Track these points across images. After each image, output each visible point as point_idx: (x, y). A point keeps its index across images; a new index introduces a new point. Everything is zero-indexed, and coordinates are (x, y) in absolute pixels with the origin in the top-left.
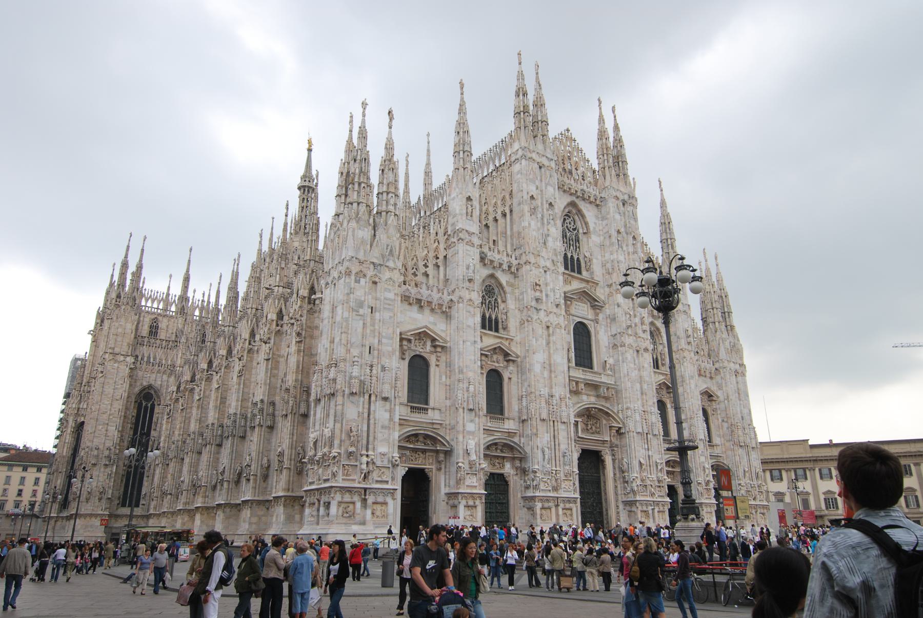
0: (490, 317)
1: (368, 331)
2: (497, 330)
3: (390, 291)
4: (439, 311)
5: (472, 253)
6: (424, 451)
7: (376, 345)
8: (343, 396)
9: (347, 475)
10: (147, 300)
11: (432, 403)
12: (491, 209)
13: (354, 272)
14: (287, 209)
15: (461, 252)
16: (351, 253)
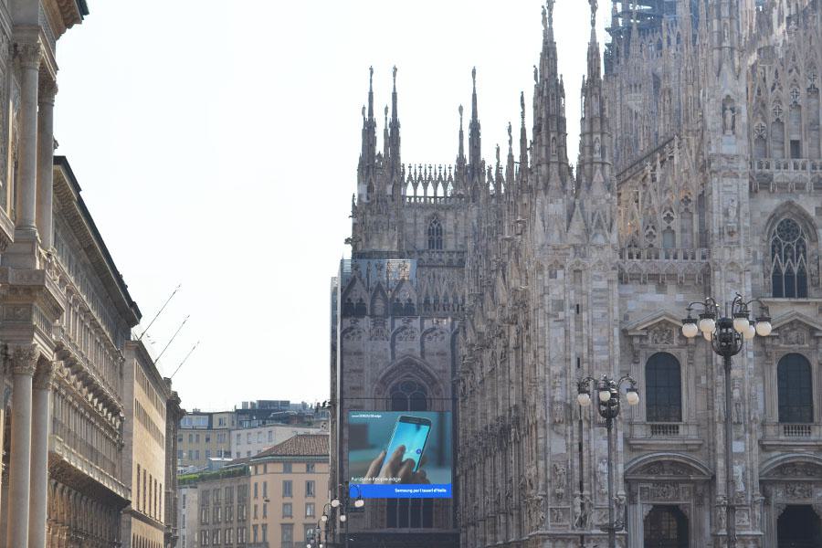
0: (789, 271)
1: (573, 340)
2: (803, 294)
3: (600, 278)
4: (689, 283)
5: (734, 189)
6: (675, 483)
7: (585, 356)
8: (545, 427)
9: (557, 520)
10: (415, 186)
11: (684, 419)
12: (785, 93)
13: (546, 266)
14: (523, 105)
15: (715, 192)
16: (540, 240)
